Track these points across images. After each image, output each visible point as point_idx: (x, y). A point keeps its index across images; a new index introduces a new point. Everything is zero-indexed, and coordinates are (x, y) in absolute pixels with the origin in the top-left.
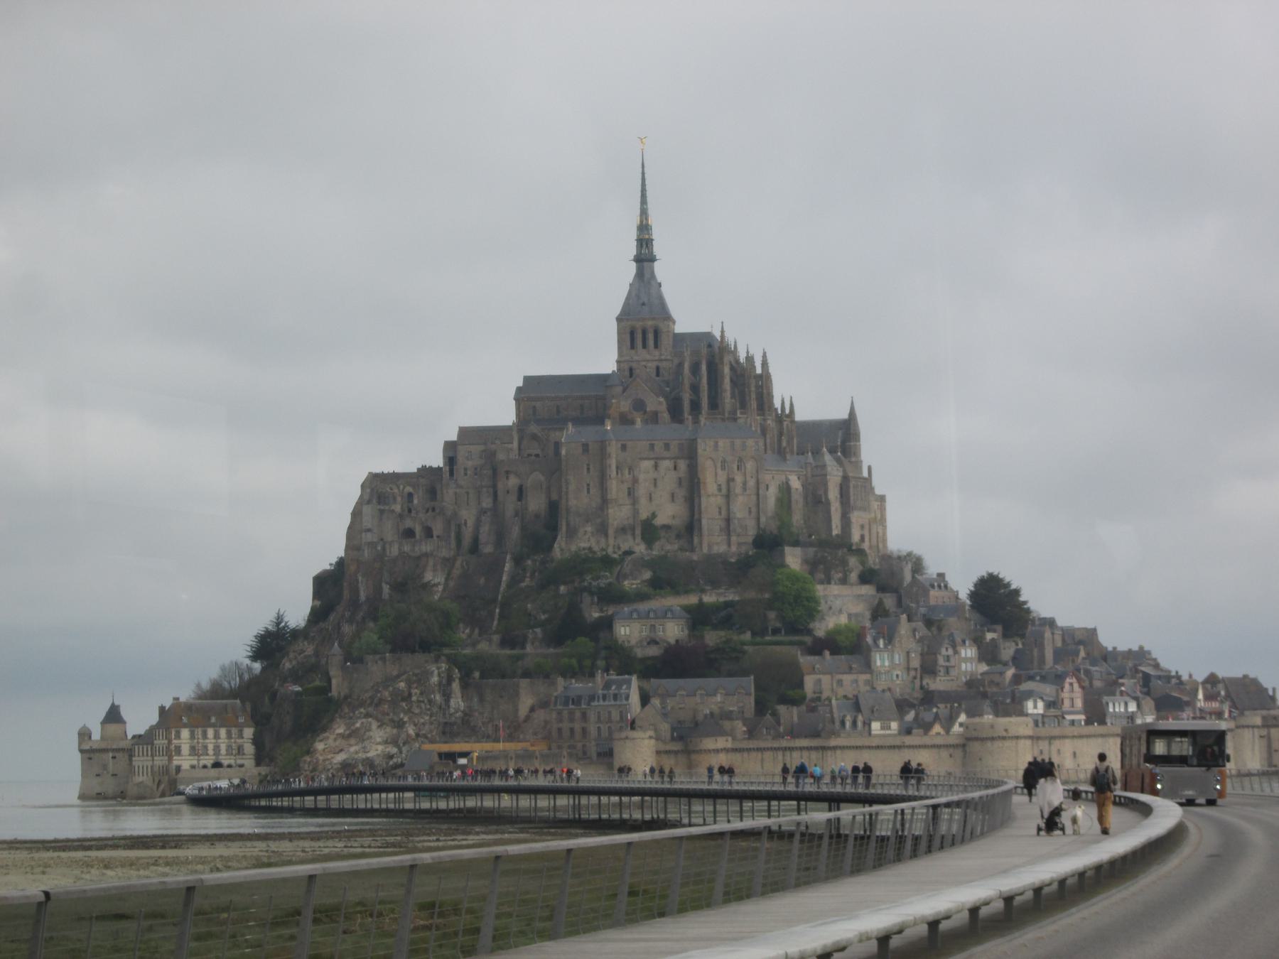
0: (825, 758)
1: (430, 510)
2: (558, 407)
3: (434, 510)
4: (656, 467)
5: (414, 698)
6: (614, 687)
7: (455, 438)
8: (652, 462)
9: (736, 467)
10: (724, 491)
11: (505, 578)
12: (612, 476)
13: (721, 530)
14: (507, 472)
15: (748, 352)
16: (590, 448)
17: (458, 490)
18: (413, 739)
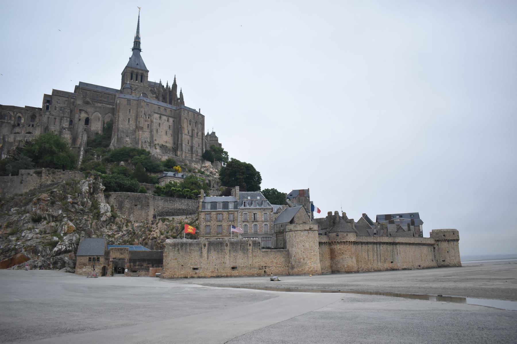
0: (393, 250)
1: (31, 126)
2: (97, 95)
3: (33, 126)
4: (160, 118)
5: (70, 200)
6: (249, 198)
7: (51, 94)
8: (159, 115)
9: (195, 125)
10: (190, 134)
11: (81, 157)
12: (143, 116)
13: (188, 151)
14: (81, 110)
15: (181, 91)
16: (132, 102)
17: (50, 116)
18: (74, 231)
